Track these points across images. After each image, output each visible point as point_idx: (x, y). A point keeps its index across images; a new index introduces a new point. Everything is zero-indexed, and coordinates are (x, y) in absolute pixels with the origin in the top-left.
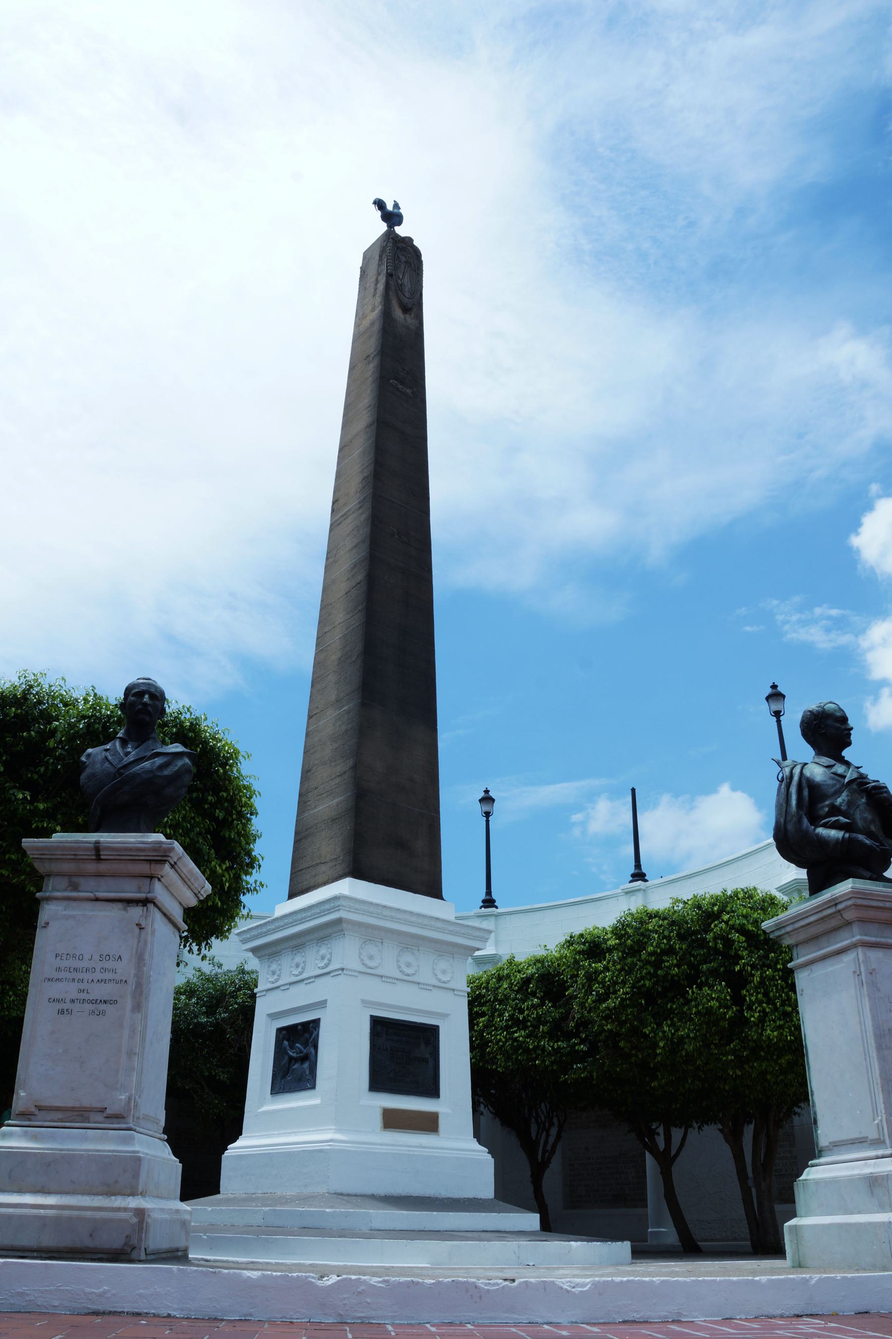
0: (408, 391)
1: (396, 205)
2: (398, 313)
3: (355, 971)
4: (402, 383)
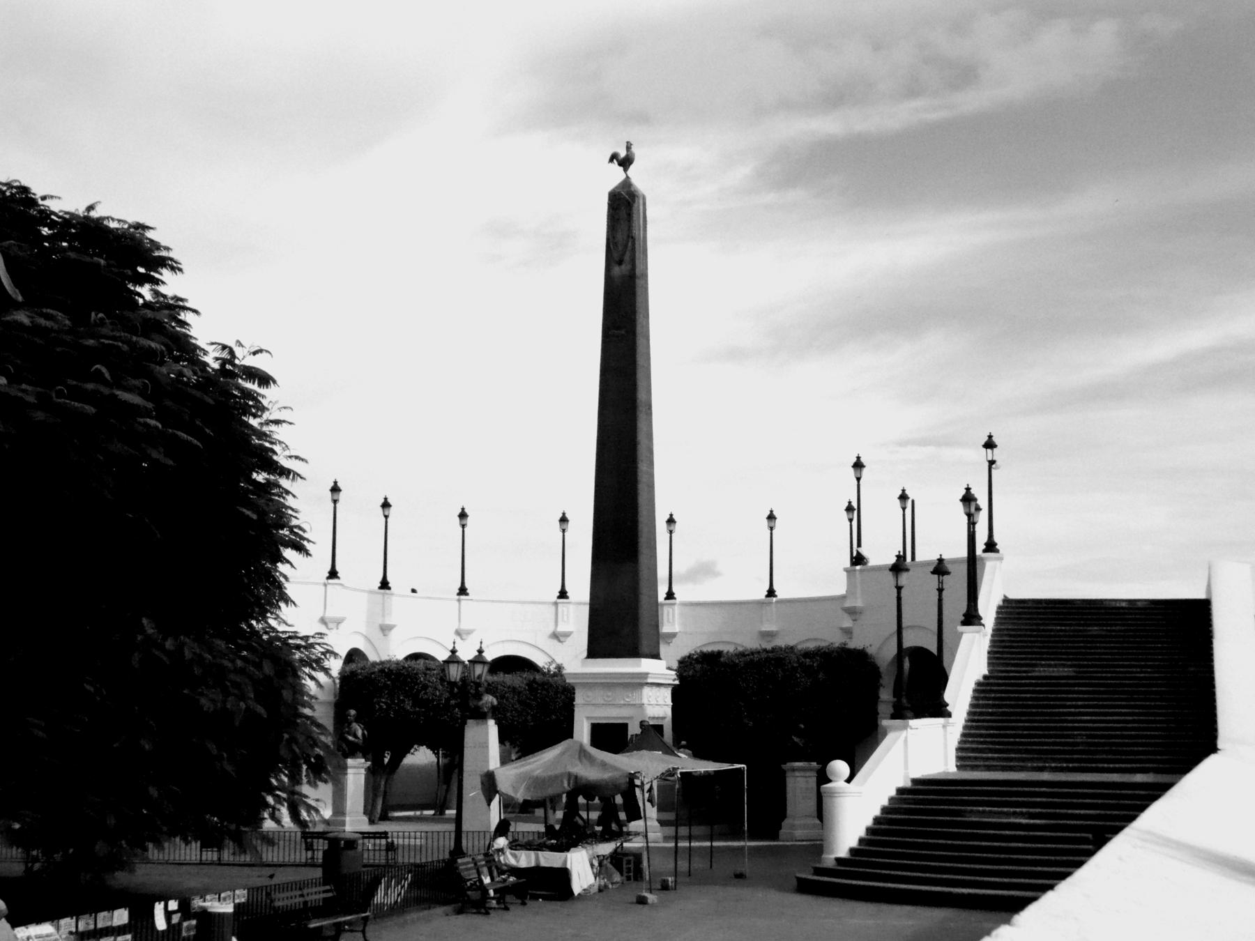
0: (623, 332)
1: (628, 147)
2: (617, 270)
4: (618, 328)
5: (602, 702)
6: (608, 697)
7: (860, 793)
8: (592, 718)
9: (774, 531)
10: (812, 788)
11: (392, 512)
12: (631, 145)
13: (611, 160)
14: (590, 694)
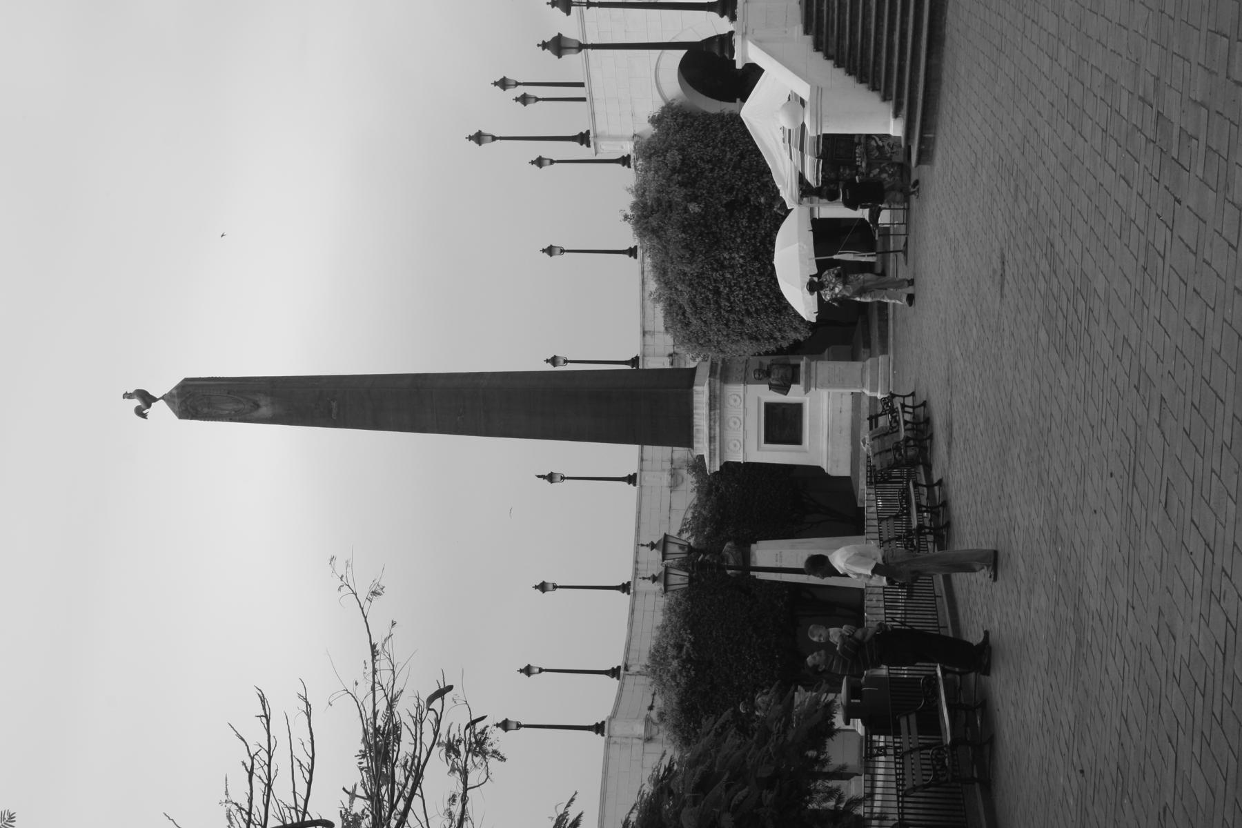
0: (334, 404)
1: (128, 396)
2: (265, 411)
4: (330, 411)
5: (742, 429)
6: (735, 423)
7: (818, 87)
9: (565, 249)
11: (536, 664)
12: (126, 393)
13: (144, 416)
14: (731, 446)
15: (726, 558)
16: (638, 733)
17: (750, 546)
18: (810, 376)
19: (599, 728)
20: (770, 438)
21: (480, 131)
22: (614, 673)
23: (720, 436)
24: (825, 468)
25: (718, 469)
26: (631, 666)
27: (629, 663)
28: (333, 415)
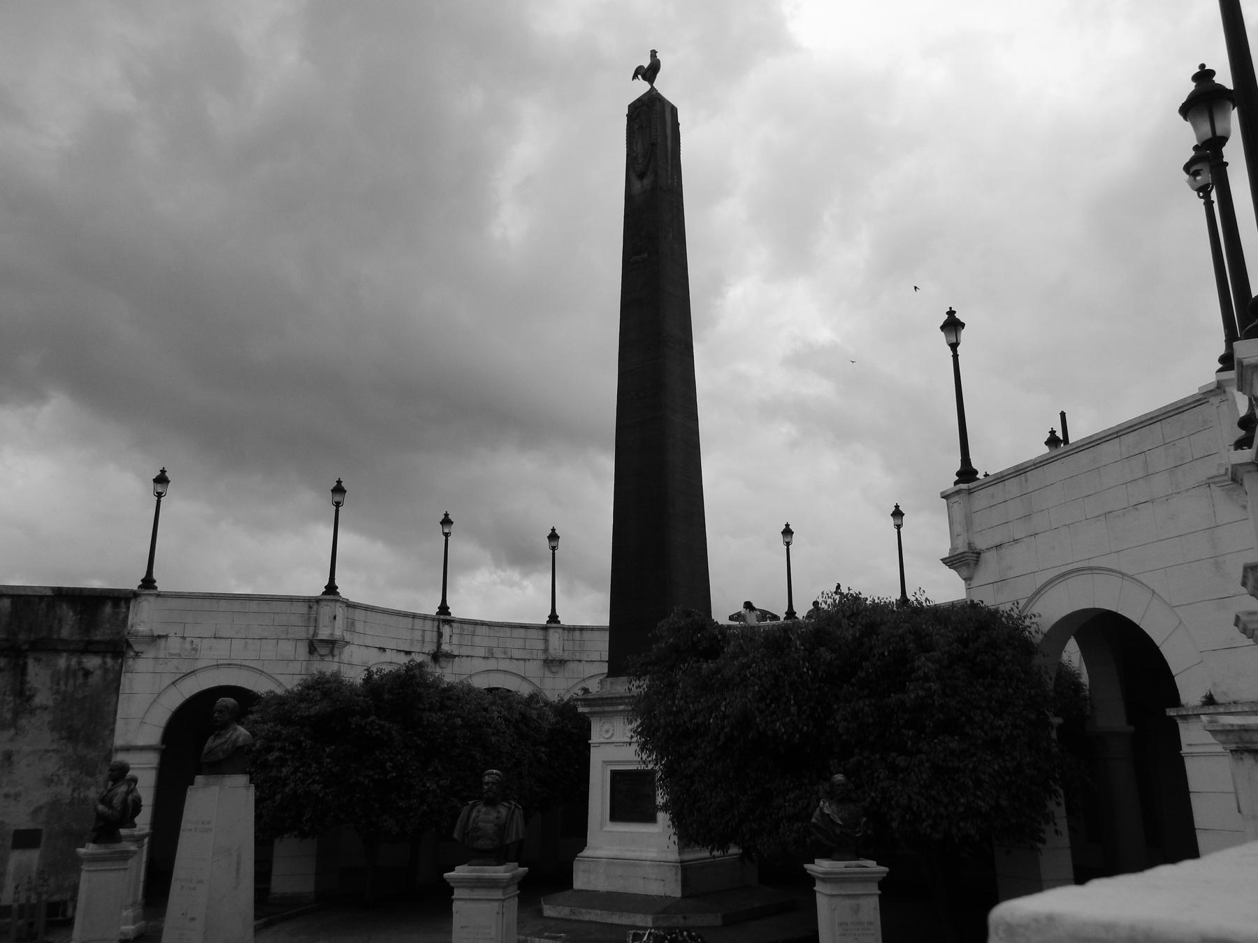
0: (645, 255)
1: (654, 53)
3: (597, 743)
8: (607, 763)
10: (870, 923)
13: (635, 76)
14: (606, 727)
15: (223, 732)
16: (320, 632)
17: (244, 772)
18: (476, 887)
19: (331, 589)
20: (618, 778)
21: (963, 325)
22: (444, 609)
23: (612, 712)
24: (586, 853)
25: (580, 710)
26: (451, 626)
27: (454, 625)
28: (634, 258)
